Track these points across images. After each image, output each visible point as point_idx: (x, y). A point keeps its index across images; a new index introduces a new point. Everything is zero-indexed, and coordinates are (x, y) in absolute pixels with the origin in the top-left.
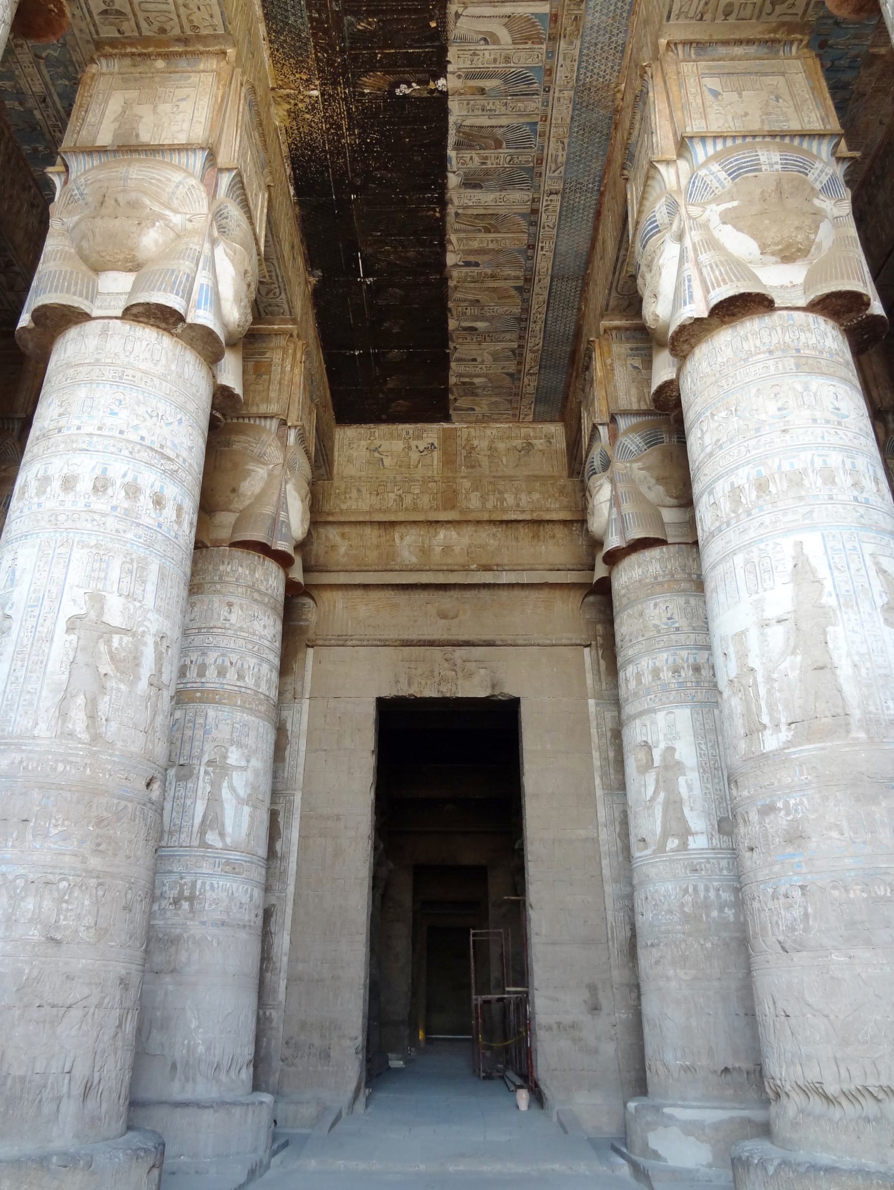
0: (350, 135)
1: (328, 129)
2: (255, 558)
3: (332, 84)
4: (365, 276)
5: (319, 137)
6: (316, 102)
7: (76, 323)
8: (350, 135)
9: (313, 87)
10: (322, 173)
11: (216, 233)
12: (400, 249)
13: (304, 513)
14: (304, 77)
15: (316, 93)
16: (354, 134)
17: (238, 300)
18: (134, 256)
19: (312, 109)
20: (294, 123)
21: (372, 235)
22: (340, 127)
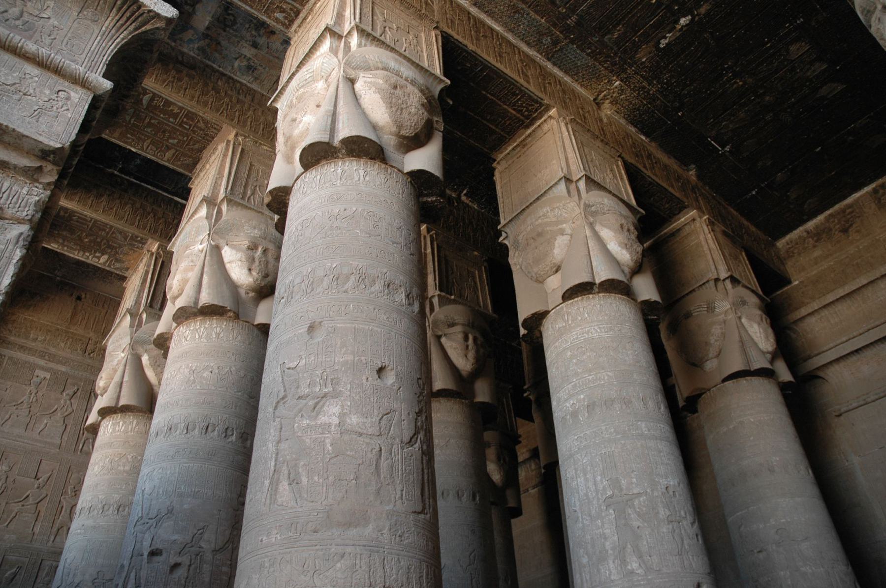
0: (653, 87)
1: (639, 93)
2: (743, 382)
3: (622, 72)
4: (723, 148)
5: (637, 101)
6: (621, 87)
7: (544, 318)
9: (614, 82)
11: (592, 220)
12: (732, 118)
13: (765, 331)
14: (606, 81)
15: (618, 83)
16: (654, 84)
17: (625, 246)
18: (554, 263)
19: (622, 91)
20: (618, 105)
21: (708, 124)
22: (644, 88)
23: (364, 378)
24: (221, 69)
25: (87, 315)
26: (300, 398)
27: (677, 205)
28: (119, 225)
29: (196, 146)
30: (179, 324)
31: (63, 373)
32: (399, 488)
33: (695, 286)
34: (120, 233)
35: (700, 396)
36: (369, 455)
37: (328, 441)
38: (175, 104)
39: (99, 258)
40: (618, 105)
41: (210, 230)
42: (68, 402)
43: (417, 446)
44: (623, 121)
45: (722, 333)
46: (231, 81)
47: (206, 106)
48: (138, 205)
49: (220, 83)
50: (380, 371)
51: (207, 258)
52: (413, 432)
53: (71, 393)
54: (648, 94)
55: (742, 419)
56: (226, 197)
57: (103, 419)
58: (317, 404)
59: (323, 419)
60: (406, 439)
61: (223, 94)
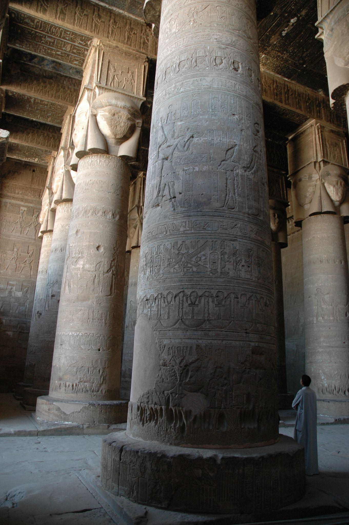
3: (264, 50)
8: (284, 55)
10: (289, 69)
15: (263, 56)
16: (285, 54)
23: (92, 251)
24: (65, 74)
25: (38, 179)
26: (72, 258)
27: (303, 117)
28: (39, 147)
29: (60, 115)
30: (57, 205)
31: (32, 207)
32: (101, 288)
33: (305, 165)
34: (40, 150)
35: (302, 221)
36: (91, 278)
37: (79, 273)
38: (44, 101)
39: (34, 160)
40: (267, 66)
41: (65, 163)
42: (36, 220)
43: (110, 273)
44: (272, 73)
45: (313, 191)
46: (70, 79)
47: (59, 98)
48: (46, 135)
49: (65, 83)
50: (98, 248)
51: (64, 177)
52: (109, 268)
53: (36, 216)
54: (283, 59)
55: (314, 236)
56: (70, 147)
57: (43, 234)
58: (77, 260)
59: (78, 266)
60: (106, 270)
61: (67, 89)
